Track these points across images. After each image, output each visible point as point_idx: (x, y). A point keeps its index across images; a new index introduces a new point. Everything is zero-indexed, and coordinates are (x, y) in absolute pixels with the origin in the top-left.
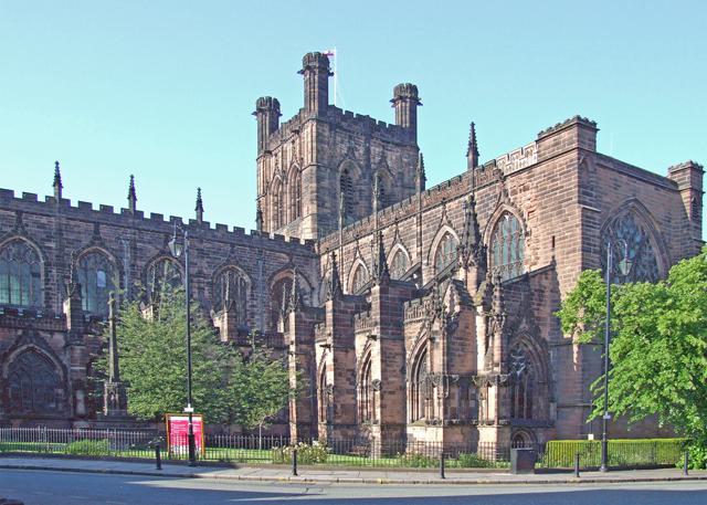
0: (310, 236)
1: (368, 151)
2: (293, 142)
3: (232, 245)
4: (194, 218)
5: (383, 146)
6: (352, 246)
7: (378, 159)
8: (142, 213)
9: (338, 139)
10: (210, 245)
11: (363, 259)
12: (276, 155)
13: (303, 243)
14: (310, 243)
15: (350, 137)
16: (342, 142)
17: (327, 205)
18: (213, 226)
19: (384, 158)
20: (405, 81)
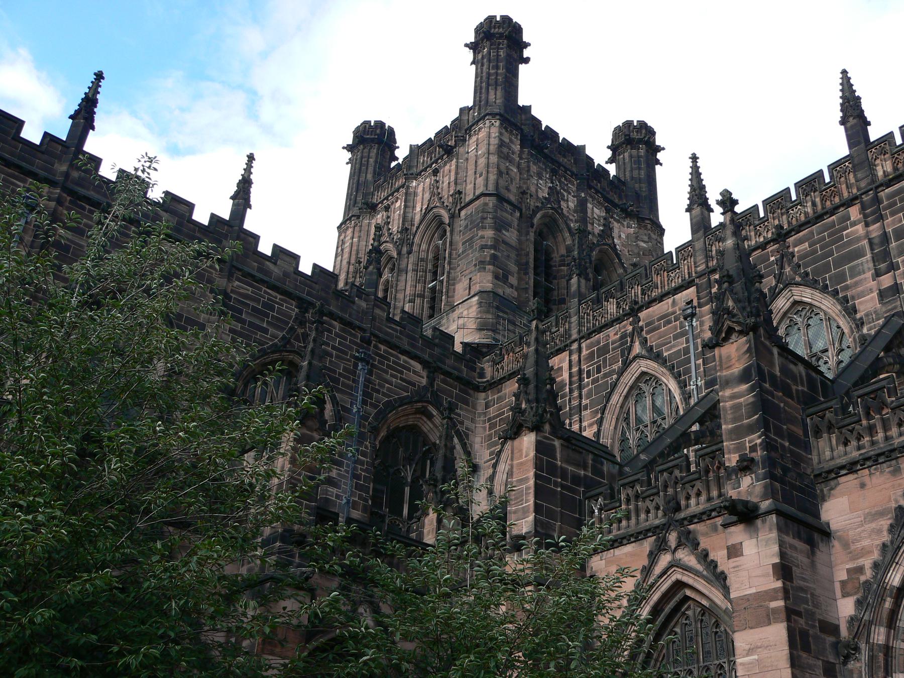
0: (474, 338)
1: (582, 206)
2: (436, 172)
3: (304, 305)
4: (226, 216)
5: (608, 211)
6: (613, 334)
7: (598, 228)
8: (97, 161)
9: (534, 168)
10: (249, 291)
11: (657, 357)
12: (387, 209)
13: (458, 348)
14: (474, 351)
15: (554, 172)
16: (540, 177)
17: (513, 280)
18: (265, 248)
19: (607, 232)
20: (635, 117)
